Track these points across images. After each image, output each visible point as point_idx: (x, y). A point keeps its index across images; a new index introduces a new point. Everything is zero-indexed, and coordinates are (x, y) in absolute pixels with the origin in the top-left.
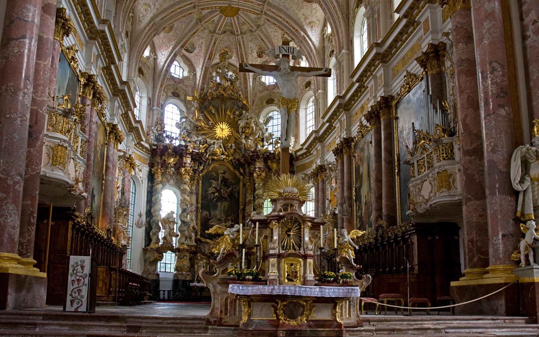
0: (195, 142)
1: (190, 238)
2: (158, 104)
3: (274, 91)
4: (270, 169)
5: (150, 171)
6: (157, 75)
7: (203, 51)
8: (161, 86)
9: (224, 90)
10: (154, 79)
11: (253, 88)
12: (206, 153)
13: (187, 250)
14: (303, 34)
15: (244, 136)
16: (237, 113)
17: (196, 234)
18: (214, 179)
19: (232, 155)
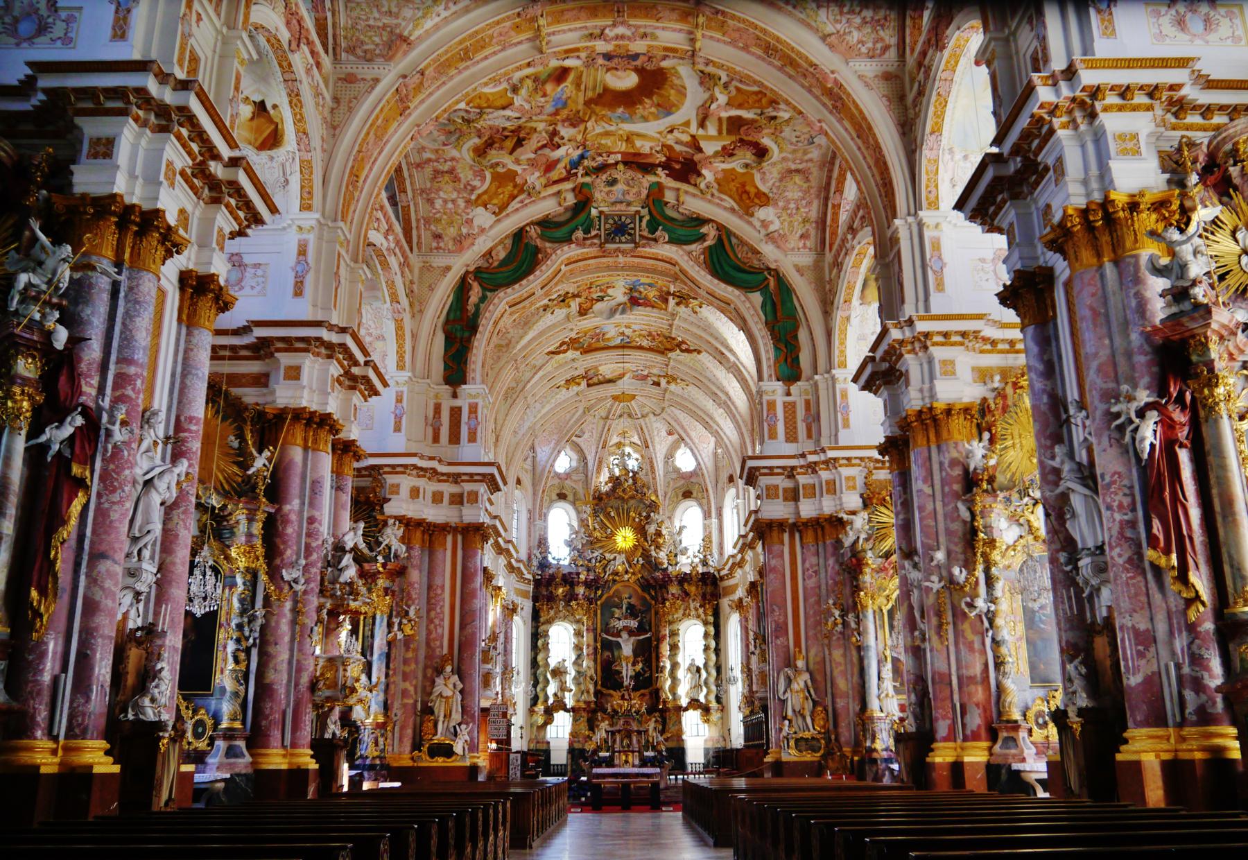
0: (590, 561)
1: (588, 692)
3: (693, 480)
4: (687, 594)
5: (534, 606)
9: (624, 491)
10: (533, 485)
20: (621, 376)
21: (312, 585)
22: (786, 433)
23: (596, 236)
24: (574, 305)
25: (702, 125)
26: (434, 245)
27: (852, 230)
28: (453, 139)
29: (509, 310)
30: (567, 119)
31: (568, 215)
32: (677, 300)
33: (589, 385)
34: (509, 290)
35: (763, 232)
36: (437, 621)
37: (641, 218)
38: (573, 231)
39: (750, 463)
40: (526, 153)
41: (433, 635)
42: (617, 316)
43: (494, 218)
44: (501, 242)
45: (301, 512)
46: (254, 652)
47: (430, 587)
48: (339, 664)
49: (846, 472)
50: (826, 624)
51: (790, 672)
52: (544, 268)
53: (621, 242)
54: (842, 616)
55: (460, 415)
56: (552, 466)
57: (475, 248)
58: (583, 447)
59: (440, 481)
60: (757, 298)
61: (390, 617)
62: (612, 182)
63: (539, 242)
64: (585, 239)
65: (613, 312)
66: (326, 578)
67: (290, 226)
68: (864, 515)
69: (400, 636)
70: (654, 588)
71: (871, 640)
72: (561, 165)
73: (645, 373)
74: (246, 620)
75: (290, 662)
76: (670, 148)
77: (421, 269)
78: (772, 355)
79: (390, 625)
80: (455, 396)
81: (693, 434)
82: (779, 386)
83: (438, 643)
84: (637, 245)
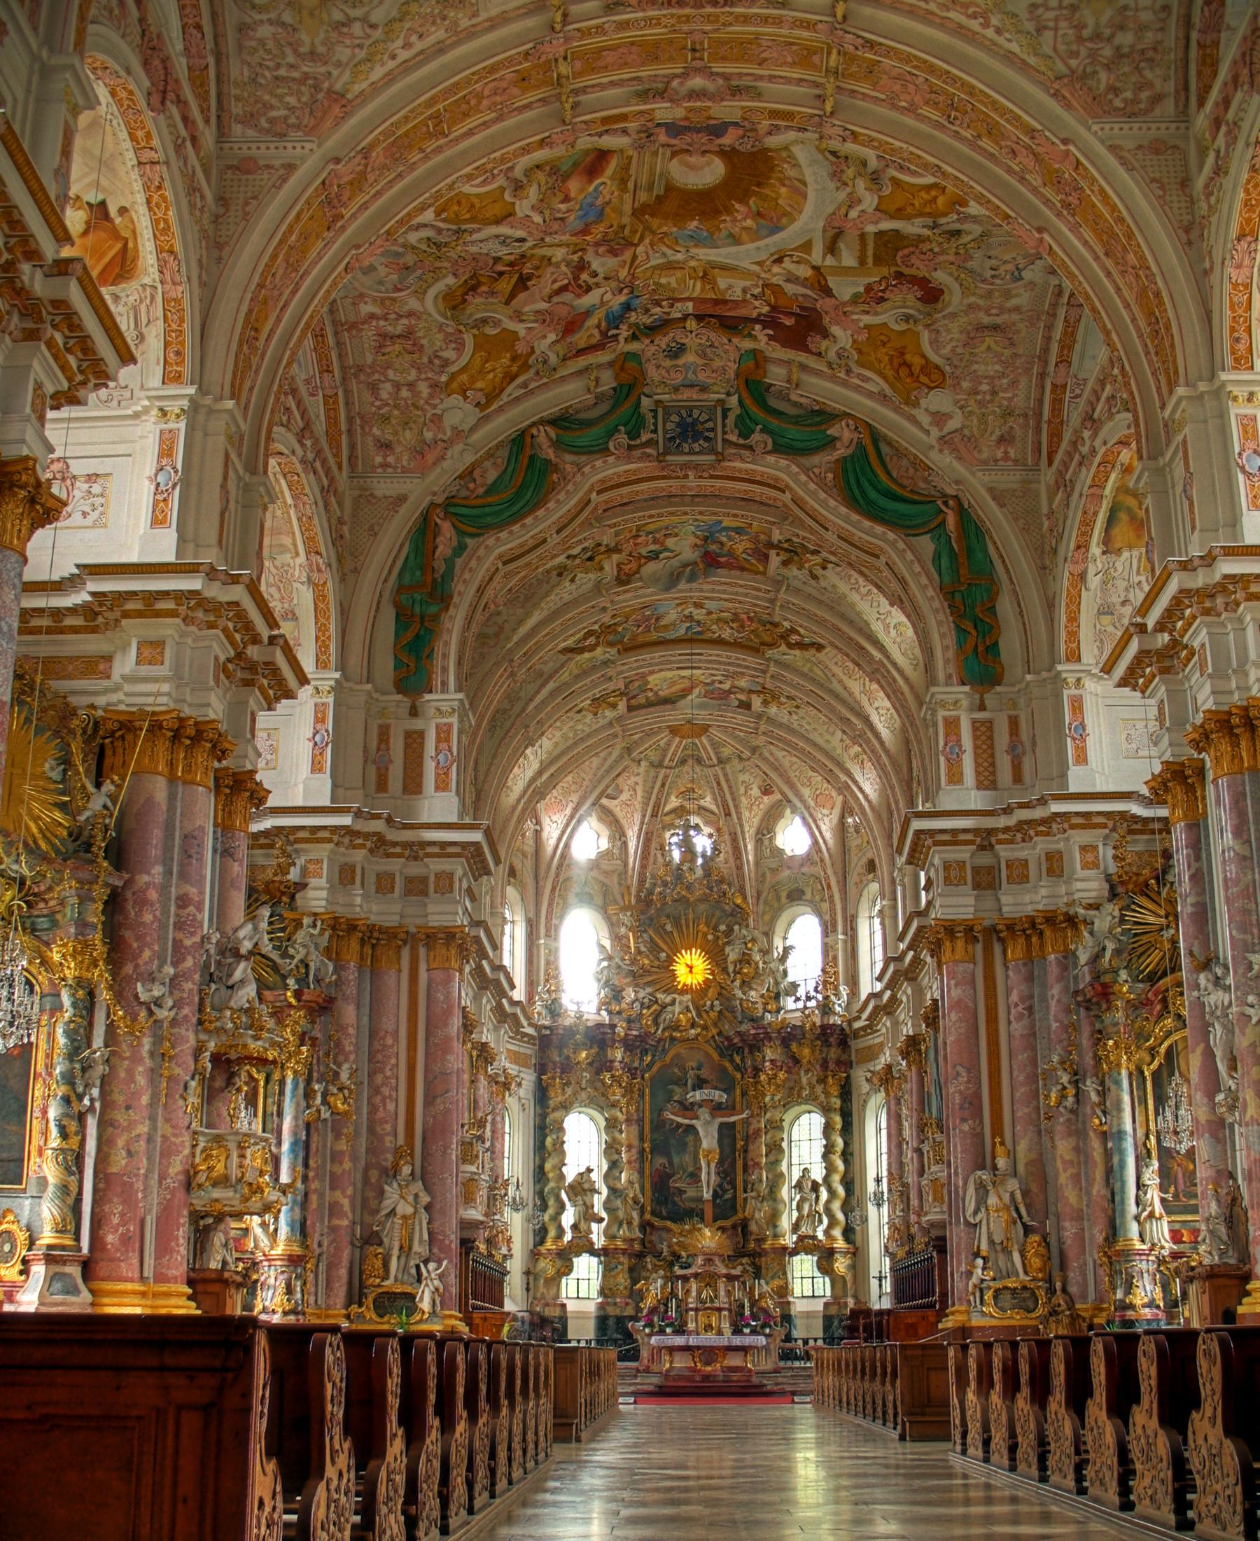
1: (630, 1223)
2: (548, 930)
4: (797, 1061)
5: (540, 1080)
6: (543, 867)
7: (639, 798)
8: (553, 889)
10: (536, 877)
11: (757, 863)
12: (656, 1023)
13: (624, 1252)
14: (843, 778)
15: (737, 983)
16: (723, 928)
17: (642, 1212)
18: (676, 1083)
19: (715, 1025)
20: (684, 693)
21: (186, 1011)
22: (978, 773)
23: (650, 443)
24: (609, 567)
25: (832, 249)
26: (379, 459)
27: (1090, 420)
28: (411, 279)
29: (503, 570)
30: (604, 241)
31: (604, 407)
32: (784, 556)
33: (631, 708)
34: (503, 535)
35: (935, 432)
36: (386, 1091)
37: (725, 413)
38: (611, 433)
39: (917, 824)
40: (533, 303)
41: (381, 1114)
42: (682, 585)
43: (477, 413)
44: (490, 455)
45: (164, 888)
46: (92, 1123)
47: (373, 1035)
48: (232, 1146)
49: (1080, 837)
50: (1047, 1097)
51: (985, 1176)
52: (562, 496)
53: (692, 452)
54: (1076, 1083)
55: (422, 745)
56: (567, 846)
57: (446, 464)
58: (617, 811)
59: (388, 855)
60: (926, 544)
61: (309, 1081)
62: (677, 351)
63: (550, 454)
64: (630, 448)
65: (673, 580)
66: (208, 1002)
67: (146, 410)
68: (1113, 909)
69: (325, 1114)
70: (739, 1050)
71: (1128, 1126)
72: (592, 321)
73: (726, 686)
74: (78, 1066)
75: (150, 1140)
76: (778, 290)
77: (356, 501)
78: (951, 641)
79: (308, 1094)
80: (414, 712)
81: (806, 792)
82: (962, 692)
83: (388, 1127)
84: (721, 457)
